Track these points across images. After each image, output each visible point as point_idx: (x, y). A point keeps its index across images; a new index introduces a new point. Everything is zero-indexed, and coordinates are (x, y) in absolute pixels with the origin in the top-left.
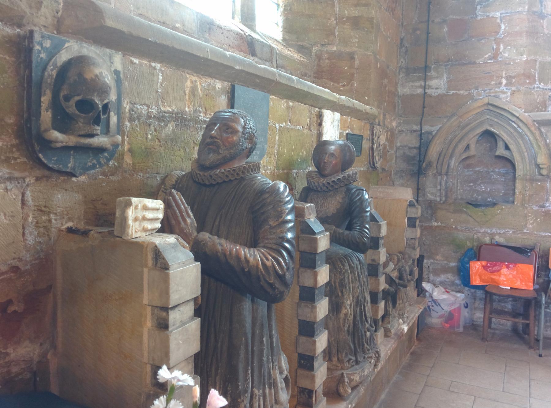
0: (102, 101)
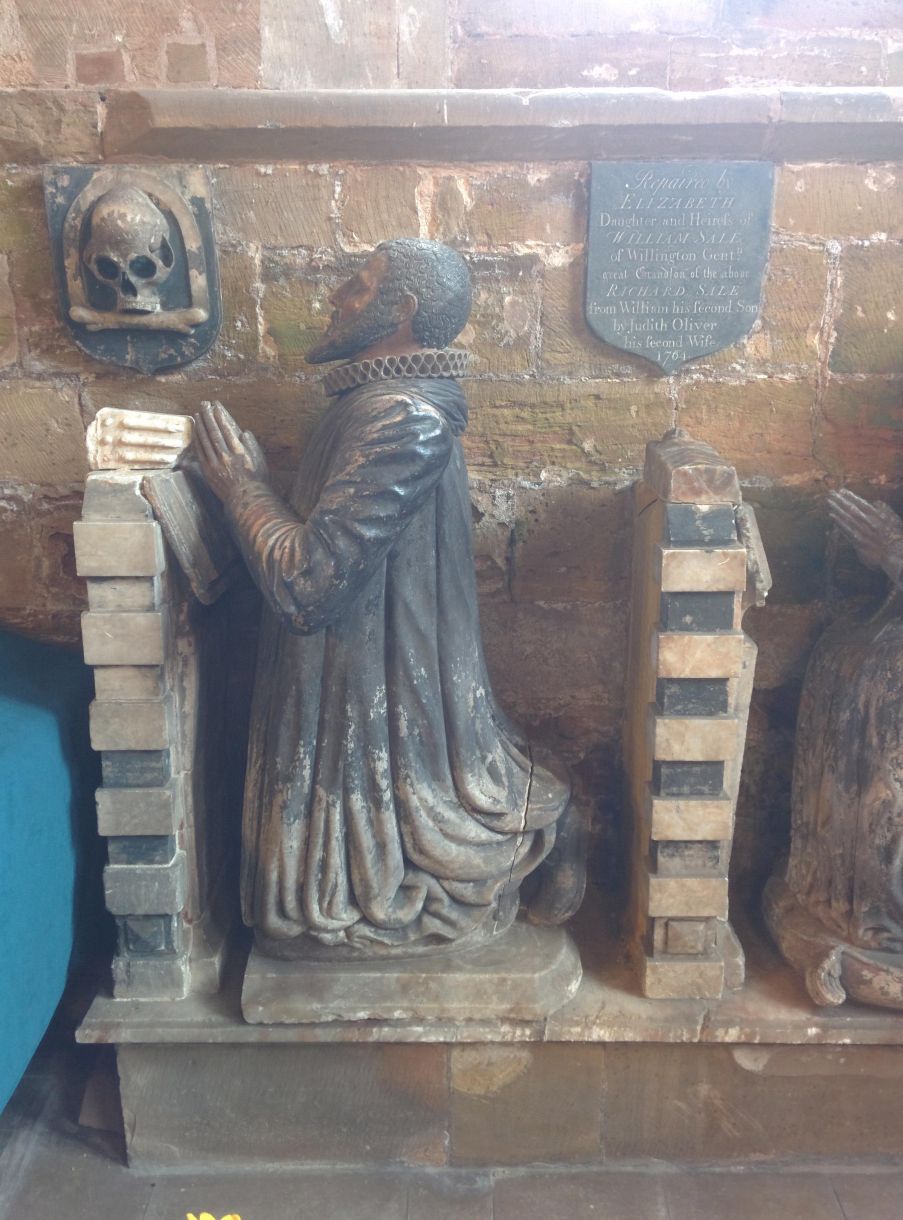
0: (124, 256)
